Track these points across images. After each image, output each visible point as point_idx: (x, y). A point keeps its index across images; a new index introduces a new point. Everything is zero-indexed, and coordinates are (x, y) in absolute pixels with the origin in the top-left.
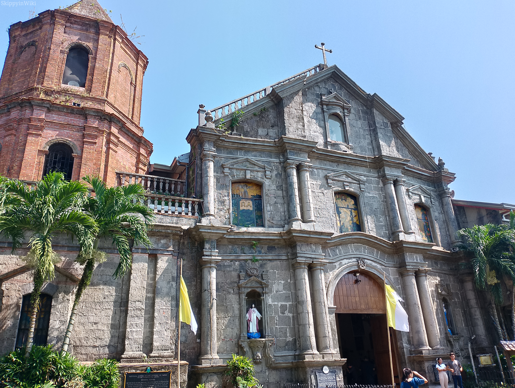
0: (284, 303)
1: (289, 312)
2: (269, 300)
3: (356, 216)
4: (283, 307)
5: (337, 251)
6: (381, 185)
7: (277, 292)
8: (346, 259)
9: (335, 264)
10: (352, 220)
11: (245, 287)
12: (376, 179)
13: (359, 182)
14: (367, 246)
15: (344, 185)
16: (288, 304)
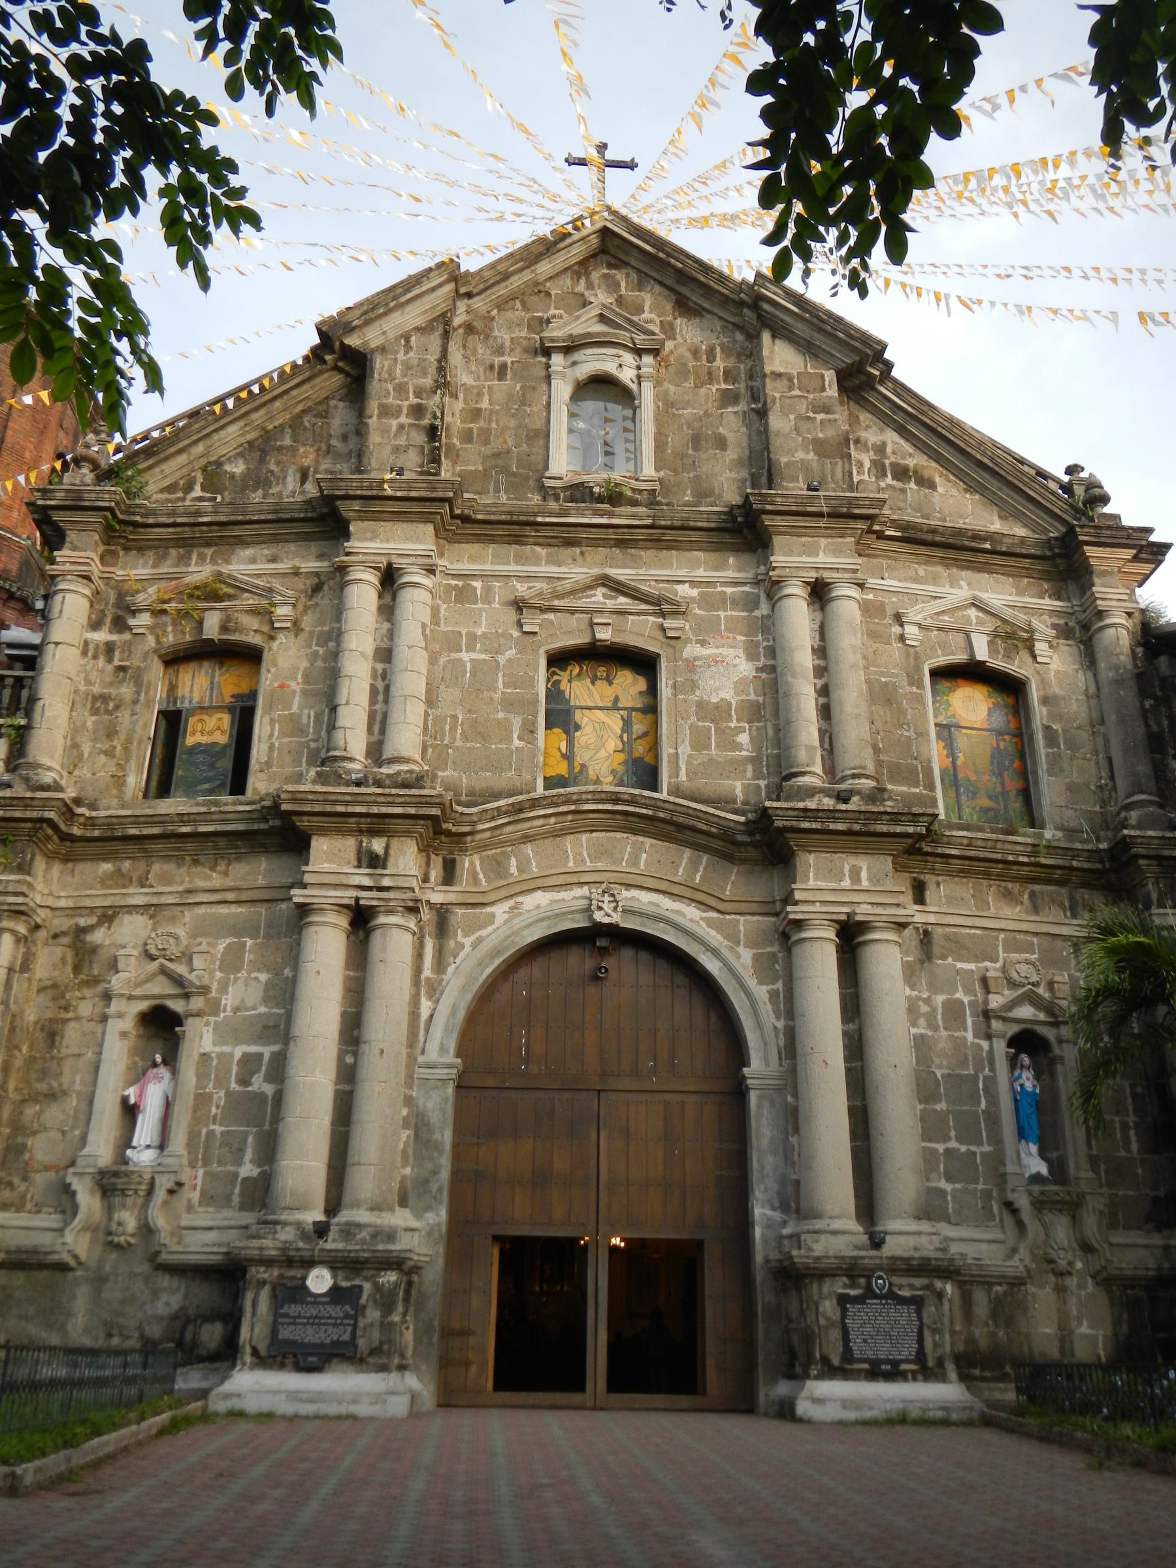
0: (253, 1049)
1: (269, 1078)
2: (200, 1038)
3: (645, 734)
4: (250, 1063)
5: (513, 862)
6: (764, 609)
7: (237, 1009)
8: (544, 888)
9: (489, 909)
10: (627, 747)
11: (130, 998)
12: (747, 589)
13: (661, 606)
14: (648, 842)
15: (592, 625)
16: (267, 1051)
